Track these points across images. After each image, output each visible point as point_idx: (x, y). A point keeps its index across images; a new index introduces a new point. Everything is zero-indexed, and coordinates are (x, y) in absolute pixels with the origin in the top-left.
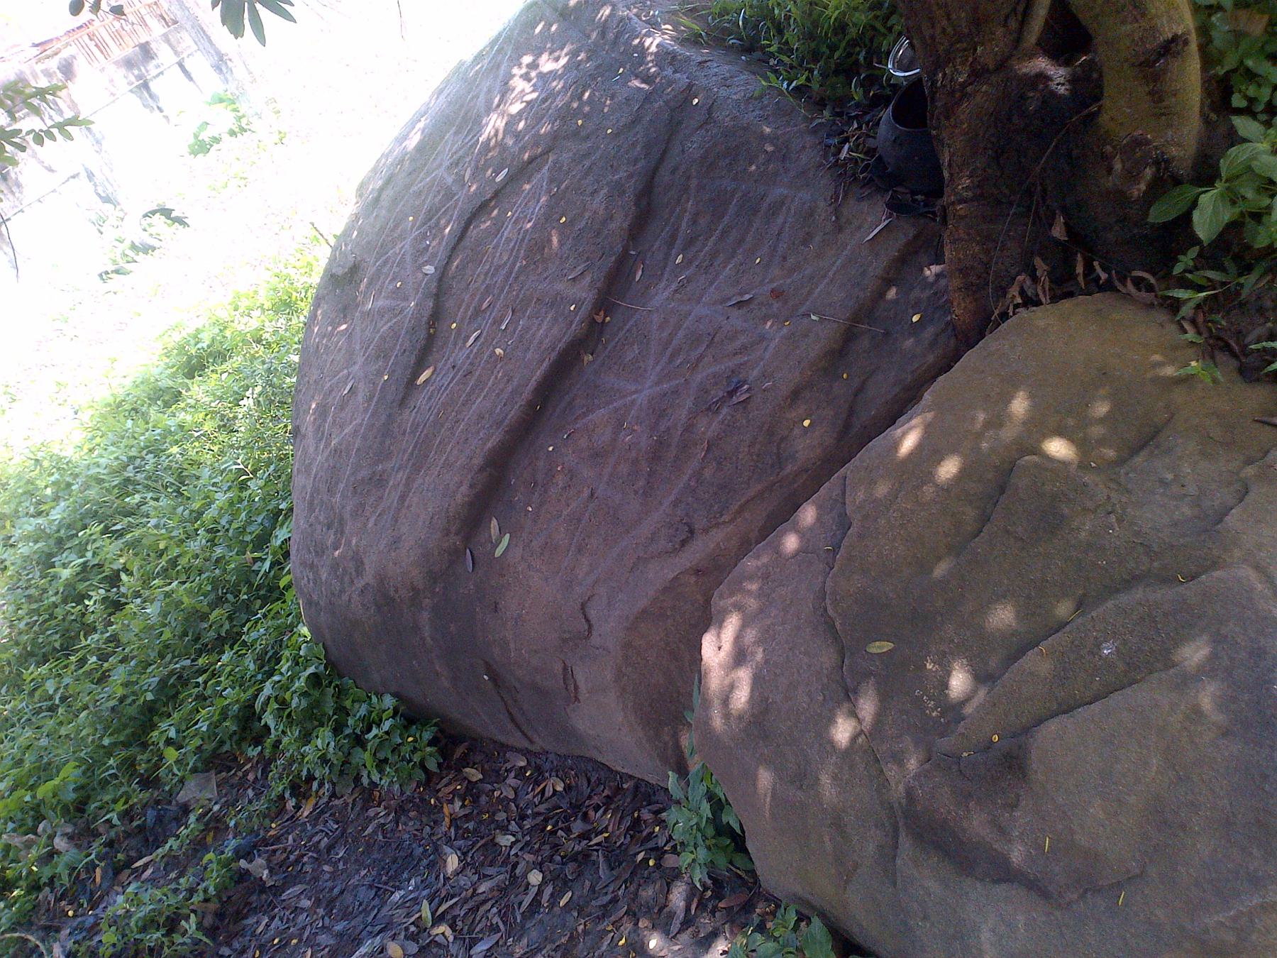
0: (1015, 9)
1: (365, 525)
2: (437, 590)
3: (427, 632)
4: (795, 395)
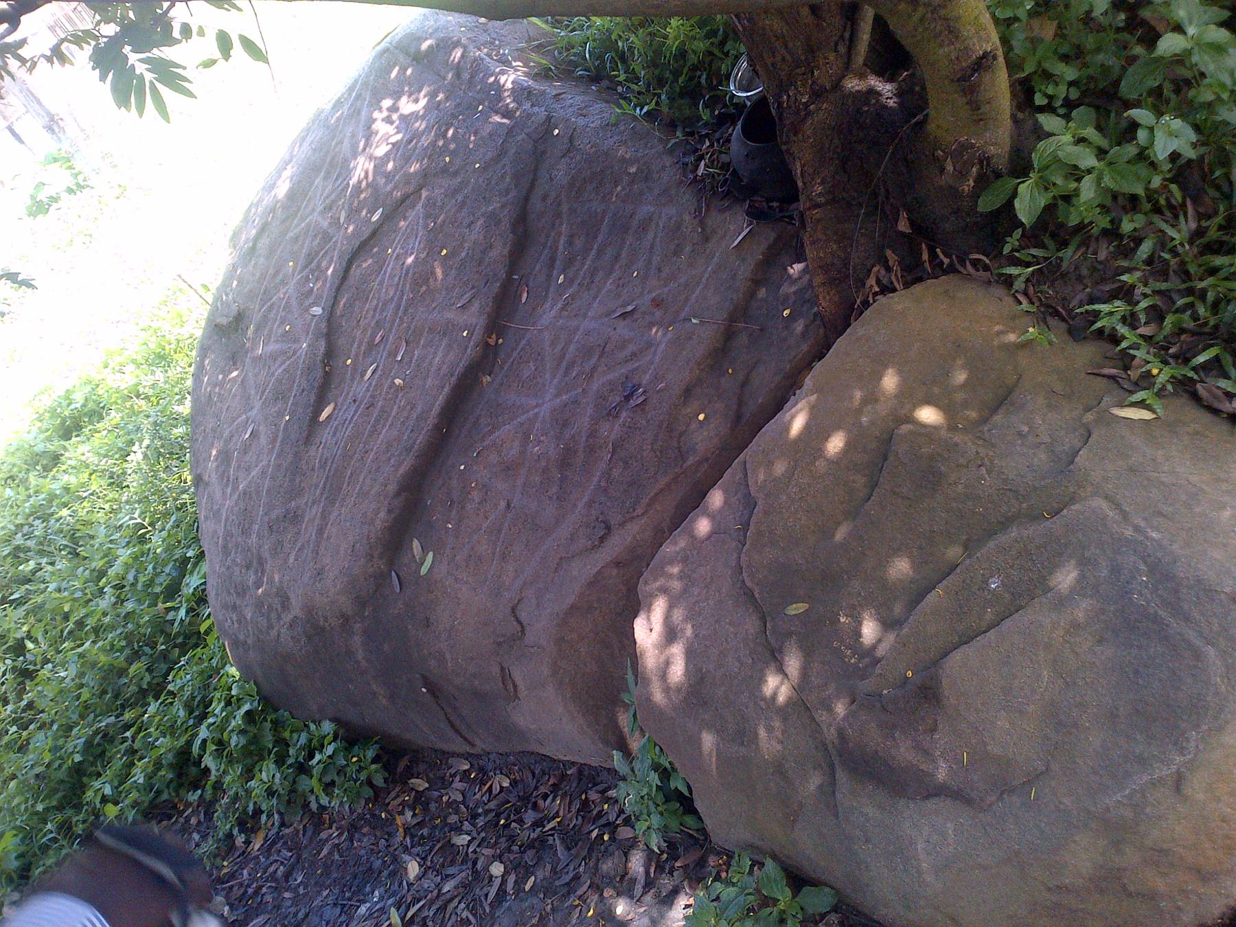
0: (842, 37)
1: (286, 561)
3: (360, 655)
4: (688, 392)
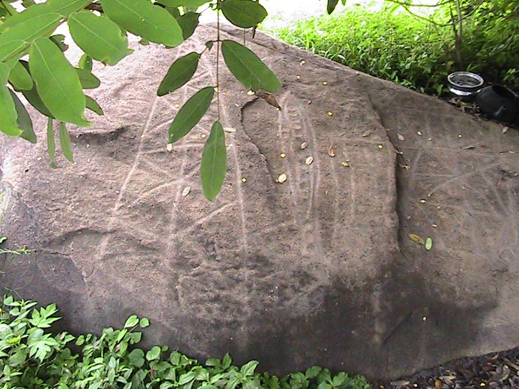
2: (386, 276)
3: (377, 306)
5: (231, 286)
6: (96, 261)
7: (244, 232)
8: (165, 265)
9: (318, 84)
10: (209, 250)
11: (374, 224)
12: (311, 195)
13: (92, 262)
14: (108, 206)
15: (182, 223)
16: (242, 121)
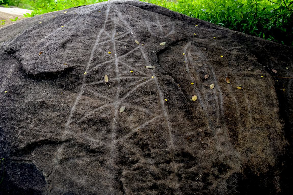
5: (165, 177)
6: (54, 164)
7: (171, 136)
8: (110, 163)
9: (209, 38)
10: (145, 150)
11: (268, 127)
12: (218, 109)
13: (51, 165)
14: (62, 123)
15: (121, 132)
16: (158, 62)
